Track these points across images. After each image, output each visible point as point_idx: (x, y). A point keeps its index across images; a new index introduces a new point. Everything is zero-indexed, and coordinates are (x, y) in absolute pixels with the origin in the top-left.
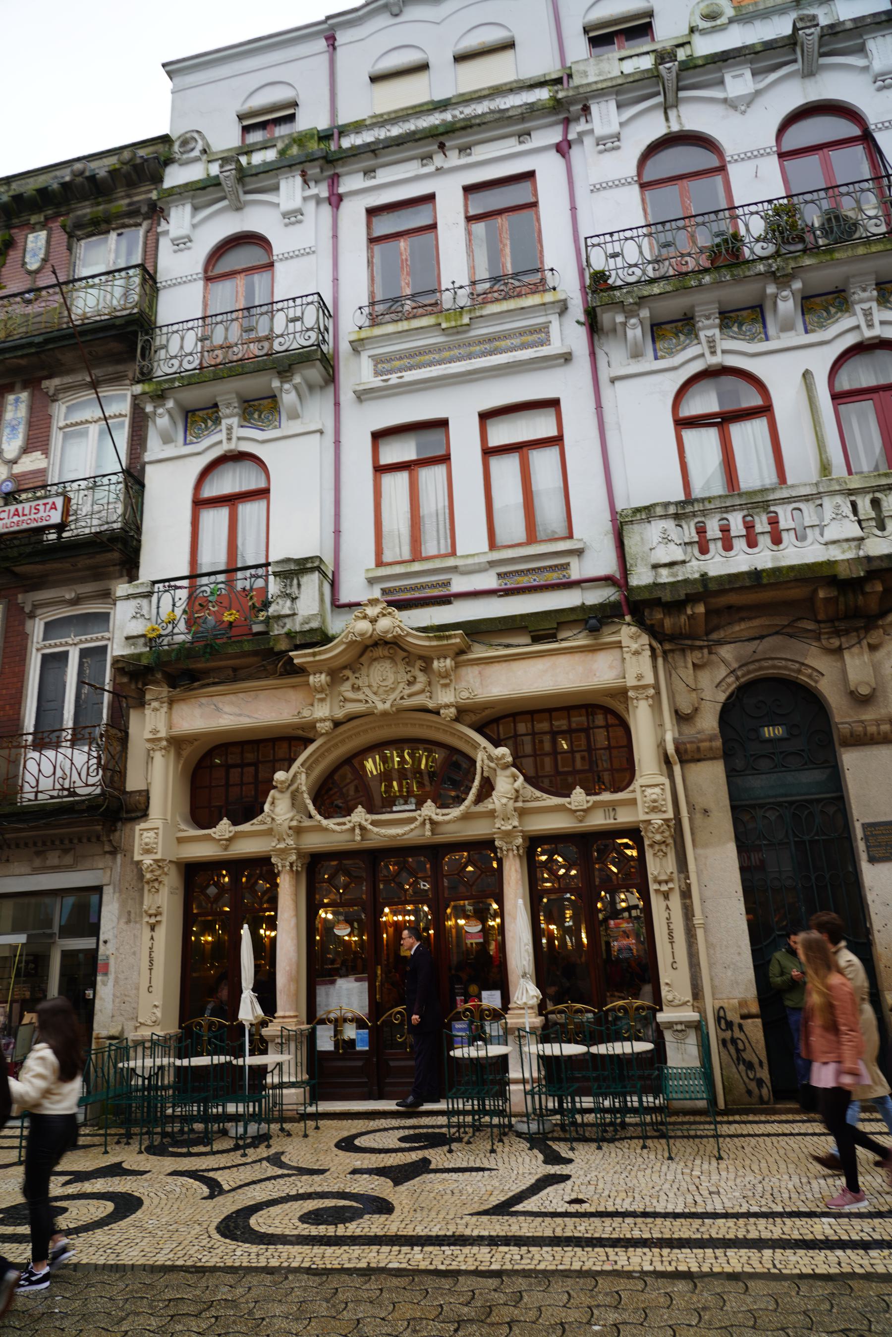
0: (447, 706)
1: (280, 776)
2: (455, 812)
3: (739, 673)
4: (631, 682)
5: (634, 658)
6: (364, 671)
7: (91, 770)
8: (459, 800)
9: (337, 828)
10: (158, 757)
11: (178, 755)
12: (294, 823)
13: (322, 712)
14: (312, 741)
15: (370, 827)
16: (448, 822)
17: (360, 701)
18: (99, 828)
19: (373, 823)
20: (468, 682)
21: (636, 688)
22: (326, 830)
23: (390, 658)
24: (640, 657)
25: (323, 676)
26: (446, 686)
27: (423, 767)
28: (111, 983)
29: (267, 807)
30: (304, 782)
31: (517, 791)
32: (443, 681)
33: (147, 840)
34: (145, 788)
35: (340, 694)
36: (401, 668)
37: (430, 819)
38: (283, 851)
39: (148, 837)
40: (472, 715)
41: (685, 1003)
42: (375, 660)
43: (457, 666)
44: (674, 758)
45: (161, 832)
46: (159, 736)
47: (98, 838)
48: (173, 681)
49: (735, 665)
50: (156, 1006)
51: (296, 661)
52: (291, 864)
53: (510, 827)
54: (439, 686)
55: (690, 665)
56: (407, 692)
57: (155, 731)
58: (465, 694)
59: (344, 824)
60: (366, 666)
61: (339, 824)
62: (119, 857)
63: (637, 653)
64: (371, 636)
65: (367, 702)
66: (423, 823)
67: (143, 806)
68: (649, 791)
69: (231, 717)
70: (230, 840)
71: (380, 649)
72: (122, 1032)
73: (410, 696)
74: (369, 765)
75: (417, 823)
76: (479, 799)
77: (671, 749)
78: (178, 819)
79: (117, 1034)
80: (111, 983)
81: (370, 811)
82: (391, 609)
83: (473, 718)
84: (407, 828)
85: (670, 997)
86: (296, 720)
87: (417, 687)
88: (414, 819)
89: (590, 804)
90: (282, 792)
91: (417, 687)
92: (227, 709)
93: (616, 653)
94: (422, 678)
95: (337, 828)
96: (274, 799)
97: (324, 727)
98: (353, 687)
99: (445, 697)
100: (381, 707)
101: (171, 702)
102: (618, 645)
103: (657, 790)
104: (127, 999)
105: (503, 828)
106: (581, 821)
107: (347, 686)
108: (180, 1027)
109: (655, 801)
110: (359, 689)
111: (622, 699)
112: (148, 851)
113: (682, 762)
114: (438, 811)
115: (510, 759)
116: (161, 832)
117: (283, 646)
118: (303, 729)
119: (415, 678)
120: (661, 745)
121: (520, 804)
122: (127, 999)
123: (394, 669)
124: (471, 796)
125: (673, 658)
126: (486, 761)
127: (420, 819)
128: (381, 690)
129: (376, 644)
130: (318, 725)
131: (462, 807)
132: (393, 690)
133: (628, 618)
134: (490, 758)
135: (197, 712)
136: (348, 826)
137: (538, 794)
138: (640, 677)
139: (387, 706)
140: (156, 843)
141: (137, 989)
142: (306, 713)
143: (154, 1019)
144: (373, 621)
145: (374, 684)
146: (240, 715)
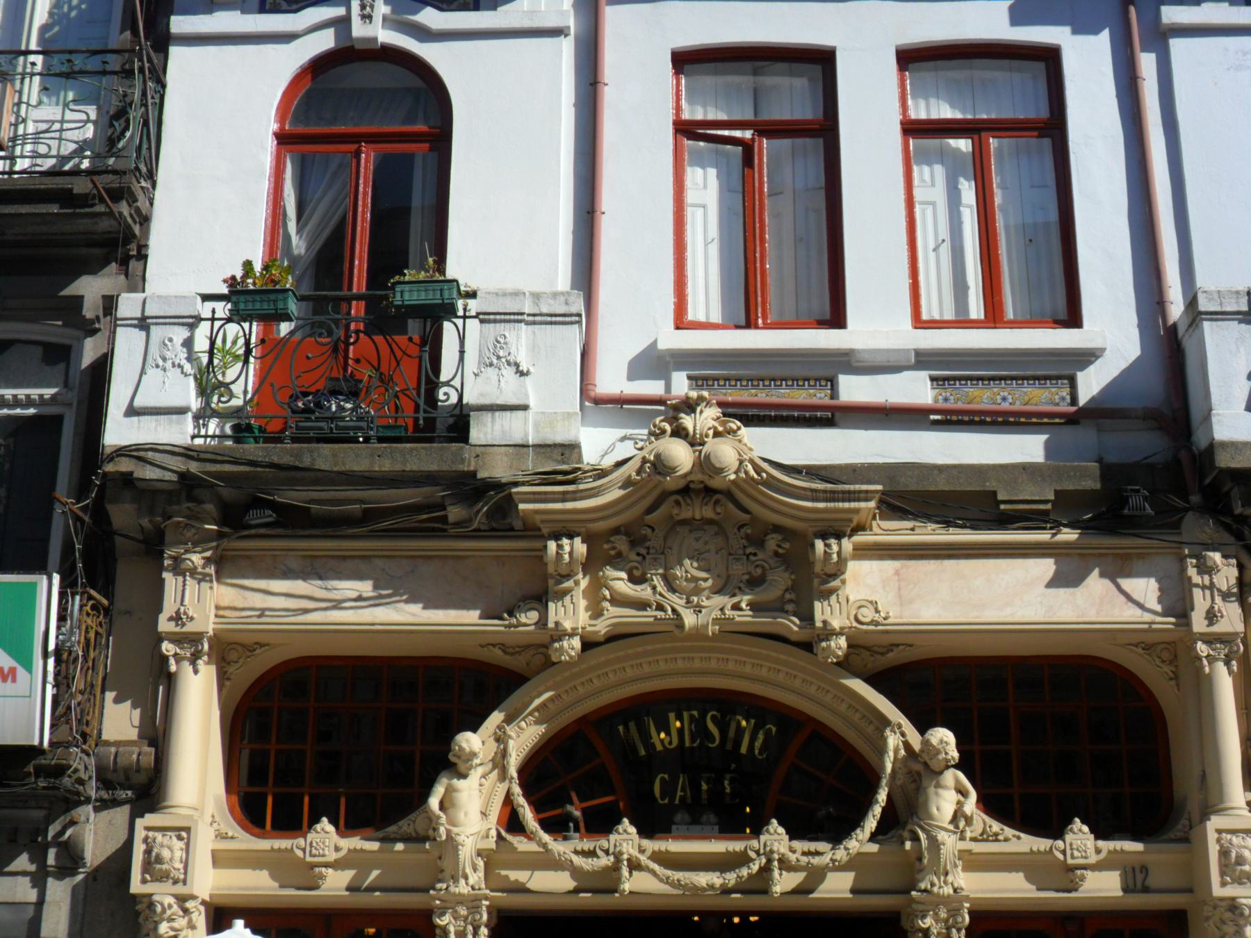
9: (578, 861)
19: (657, 857)
21: (1210, 640)
25: (578, 540)
27: (744, 750)
40: (866, 654)
46: (190, 628)
48: (234, 518)
51: (521, 506)
53: (948, 890)
58: (867, 614)
59: (592, 854)
64: (686, 475)
65: (660, 607)
66: (766, 870)
81: (646, 831)
82: (734, 424)
84: (731, 878)
88: (742, 859)
89: (1103, 855)
111: (1166, 655)
115: (954, 754)
117: (498, 469)
118: (503, 647)
124: (871, 824)
133: (1195, 499)
137: (996, 826)
144: (695, 442)
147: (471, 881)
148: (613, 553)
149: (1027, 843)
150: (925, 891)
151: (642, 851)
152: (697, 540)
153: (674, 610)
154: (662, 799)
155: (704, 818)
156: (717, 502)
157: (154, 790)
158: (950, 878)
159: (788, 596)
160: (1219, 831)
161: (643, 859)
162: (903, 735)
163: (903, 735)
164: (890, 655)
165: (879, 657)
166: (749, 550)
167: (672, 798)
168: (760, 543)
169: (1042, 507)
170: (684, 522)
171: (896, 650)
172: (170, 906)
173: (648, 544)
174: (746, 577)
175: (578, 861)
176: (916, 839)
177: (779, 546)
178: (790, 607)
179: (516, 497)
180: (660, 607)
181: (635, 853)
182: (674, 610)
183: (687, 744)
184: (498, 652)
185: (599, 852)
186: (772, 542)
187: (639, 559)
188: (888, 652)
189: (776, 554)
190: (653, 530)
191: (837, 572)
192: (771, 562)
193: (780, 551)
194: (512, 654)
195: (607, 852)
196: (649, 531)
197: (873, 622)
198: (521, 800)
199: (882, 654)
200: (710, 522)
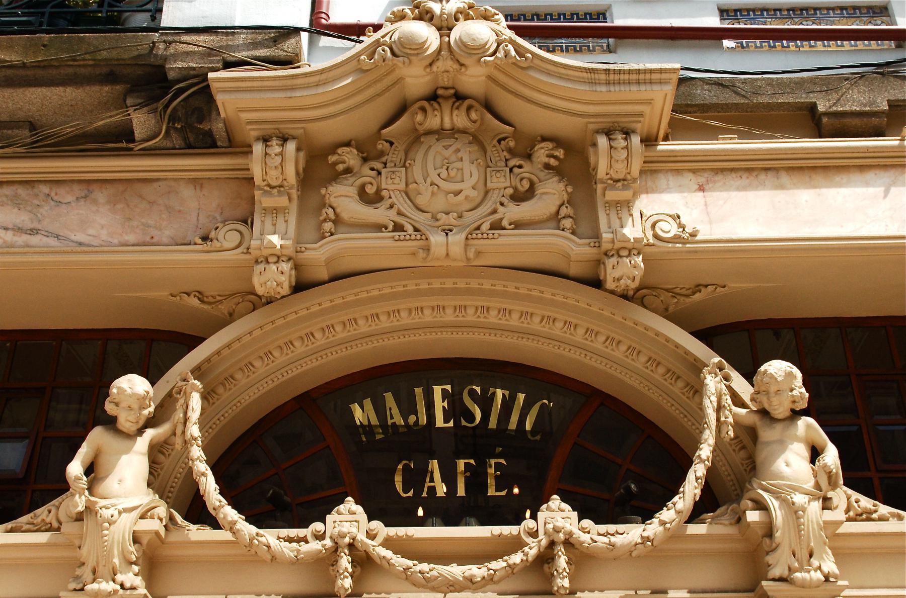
6: (395, 156)
12: (154, 525)
36: (497, 154)
37: (569, 543)
53: (818, 576)
58: (669, 229)
65: (398, 228)
71: (446, 106)
75: (532, 552)
88: (517, 544)
115: (800, 391)
119: (532, 184)
126: (727, 400)
129: (433, 97)
137: (866, 502)
146: (33, 232)
147: (119, 577)
148: (341, 167)
150: (781, 579)
151: (371, 536)
152: (446, 148)
153: (416, 230)
154: (405, 492)
156: (469, 108)
159: (564, 211)
162: (727, 378)
163: (727, 378)
164: (697, 296)
165: (682, 298)
166: (512, 163)
167: (418, 493)
168: (529, 157)
170: (429, 133)
173: (384, 159)
174: (510, 191)
176: (761, 506)
177: (549, 156)
178: (567, 223)
179: (214, 86)
180: (398, 228)
181: (361, 537)
182: (416, 230)
183: (440, 422)
184: (194, 302)
185: (309, 538)
186: (541, 153)
187: (374, 173)
188: (694, 293)
189: (547, 166)
190: (392, 144)
192: (542, 175)
193: (552, 162)
194: (210, 303)
195: (320, 537)
196: (388, 145)
197: (676, 239)
199: (687, 296)
200: (464, 132)
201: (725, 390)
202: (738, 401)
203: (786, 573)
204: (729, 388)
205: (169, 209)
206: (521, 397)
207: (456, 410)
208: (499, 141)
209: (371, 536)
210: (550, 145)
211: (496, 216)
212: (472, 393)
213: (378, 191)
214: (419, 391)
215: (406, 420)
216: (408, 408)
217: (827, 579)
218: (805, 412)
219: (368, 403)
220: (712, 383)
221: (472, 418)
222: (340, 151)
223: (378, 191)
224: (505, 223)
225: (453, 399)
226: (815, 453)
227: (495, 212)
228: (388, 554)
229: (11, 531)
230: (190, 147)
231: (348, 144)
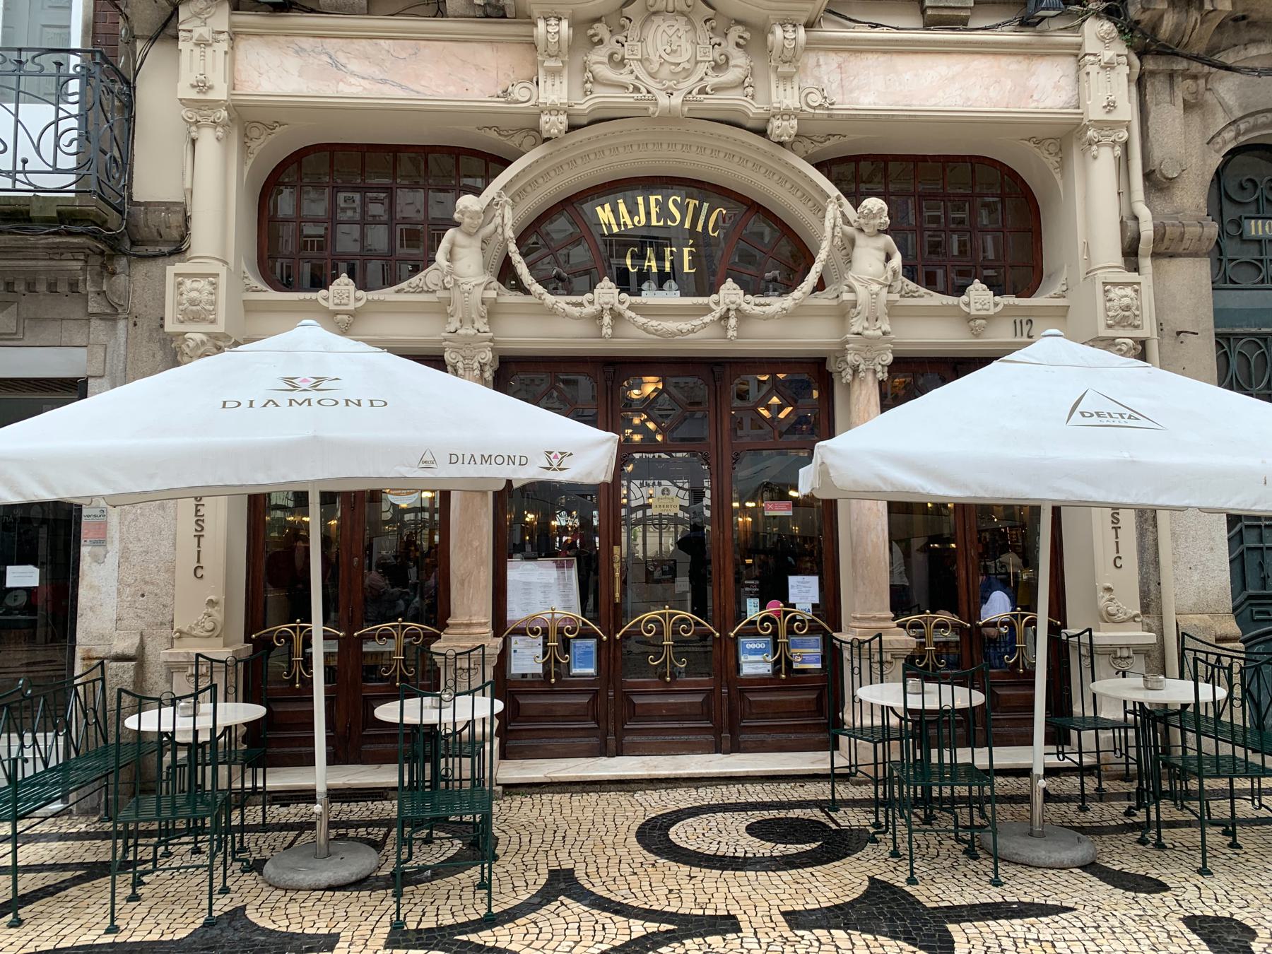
0: (786, 114)
1: (467, 202)
2: (777, 304)
3: (1242, 127)
4: (1095, 112)
5: (1102, 72)
6: (633, 30)
7: (64, 140)
8: (787, 286)
9: (569, 309)
10: (208, 140)
11: (245, 148)
12: (492, 294)
13: (556, 92)
14: (506, 163)
15: (629, 314)
16: (766, 318)
17: (624, 87)
18: (77, 265)
20: (819, 79)
22: (552, 312)
23: (682, 14)
24: (1113, 74)
25: (565, 24)
26: (786, 78)
27: (699, 229)
28: (112, 558)
29: (440, 256)
30: (509, 222)
31: (895, 272)
32: (784, 69)
33: (194, 294)
34: (178, 198)
35: (585, 68)
36: (703, 33)
38: (468, 342)
39: (196, 289)
41: (1133, 618)
42: (655, 13)
43: (811, 46)
44: (1145, 246)
45: (222, 281)
47: (73, 286)
49: (1238, 114)
50: (211, 603)
52: (482, 366)
54: (773, 77)
55: (1180, 103)
56: (712, 80)
57: (202, 86)
58: (816, 99)
59: (581, 305)
60: (637, 22)
61: (575, 305)
62: (121, 324)
63: (1109, 66)
66: (725, 317)
67: (175, 234)
68: (1116, 293)
69: (365, 83)
70: (353, 314)
72: (142, 646)
73: (716, 89)
74: (604, 214)
76: (820, 286)
77: (1147, 230)
78: (244, 268)
79: (132, 651)
80: (112, 558)
83: (812, 149)
84: (697, 322)
85: (1112, 609)
86: (500, 105)
87: (731, 75)
88: (707, 310)
90: (470, 235)
91: (731, 75)
92: (354, 66)
93: (1068, 65)
94: (739, 59)
95: (576, 311)
96: (453, 245)
97: (553, 124)
98: (611, 56)
99: (786, 97)
100: (663, 101)
101: (234, 35)
102: (1077, 54)
103: (1129, 291)
104: (148, 588)
105: (866, 332)
106: (977, 336)
107: (598, 57)
108: (247, 639)
109: (1128, 308)
110: (622, 63)
112: (196, 318)
113: (1155, 255)
114: (749, 297)
116: (222, 281)
118: (498, 129)
119: (727, 59)
120: (1129, 222)
121: (896, 297)
122: (148, 588)
123: (691, 34)
124: (812, 278)
125: (1153, 84)
126: (839, 221)
127: (718, 312)
128: (666, 70)
130: (544, 118)
131: (797, 294)
132: (688, 73)
134: (843, 215)
135: (292, 63)
136: (589, 310)
137: (913, 286)
138: (1110, 107)
139: (677, 100)
140: (213, 303)
141: (171, 570)
142: (520, 93)
143: (209, 625)
145: (655, 58)
146: (384, 82)
147: (476, 325)
148: (596, 39)
149: (937, 299)
155: (666, 285)
157: (184, 247)
158: (878, 324)
160: (1105, 284)
161: (622, 308)
166: (713, 42)
169: (963, 13)
171: (833, 141)
172: (203, 342)
175: (569, 309)
176: (852, 290)
177: (741, 37)
178: (750, 90)
181: (617, 304)
183: (654, 223)
184: (493, 134)
185: (585, 303)
186: (736, 32)
191: (791, 58)
193: (741, 41)
195: (592, 303)
198: (516, 258)
201: (839, 215)
202: (847, 222)
203: (860, 330)
204: (842, 213)
205: (477, 67)
206: (706, 205)
207: (664, 213)
208: (705, 22)
209: (622, 303)
210: (740, 28)
211: (702, 84)
212: (675, 201)
213: (623, 59)
214: (640, 200)
215: (632, 220)
216: (633, 212)
217: (884, 333)
218: (885, 232)
219: (607, 206)
220: (832, 211)
221: (674, 220)
222: (595, 26)
223: (623, 59)
224: (708, 89)
225: (663, 207)
226: (888, 258)
227: (702, 79)
228: (633, 315)
229: (398, 292)
230: (487, 16)
231: (598, 20)
